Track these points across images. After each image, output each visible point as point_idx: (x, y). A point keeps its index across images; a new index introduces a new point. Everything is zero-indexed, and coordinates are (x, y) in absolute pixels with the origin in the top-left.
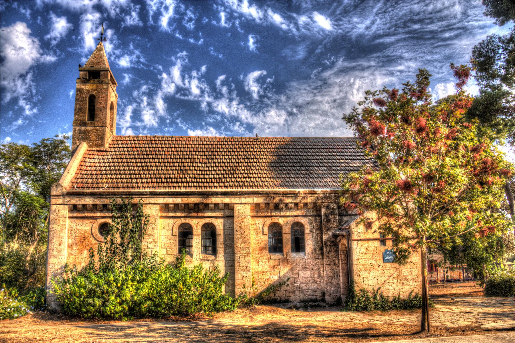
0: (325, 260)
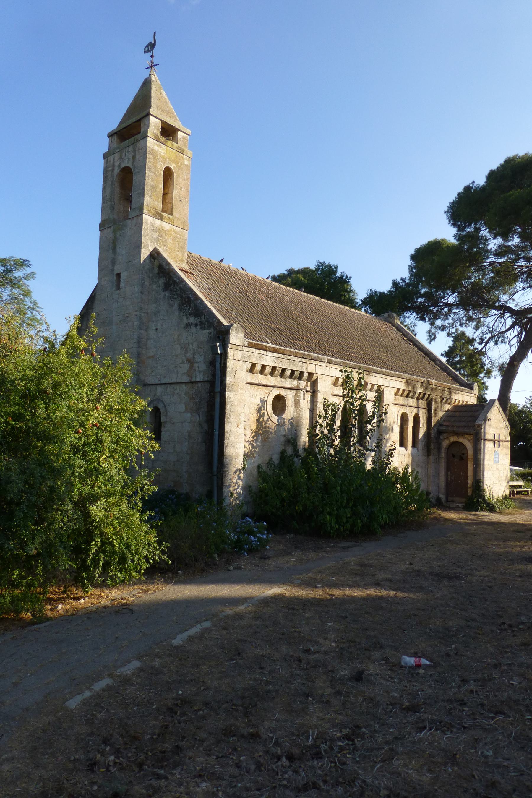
0: (432, 457)
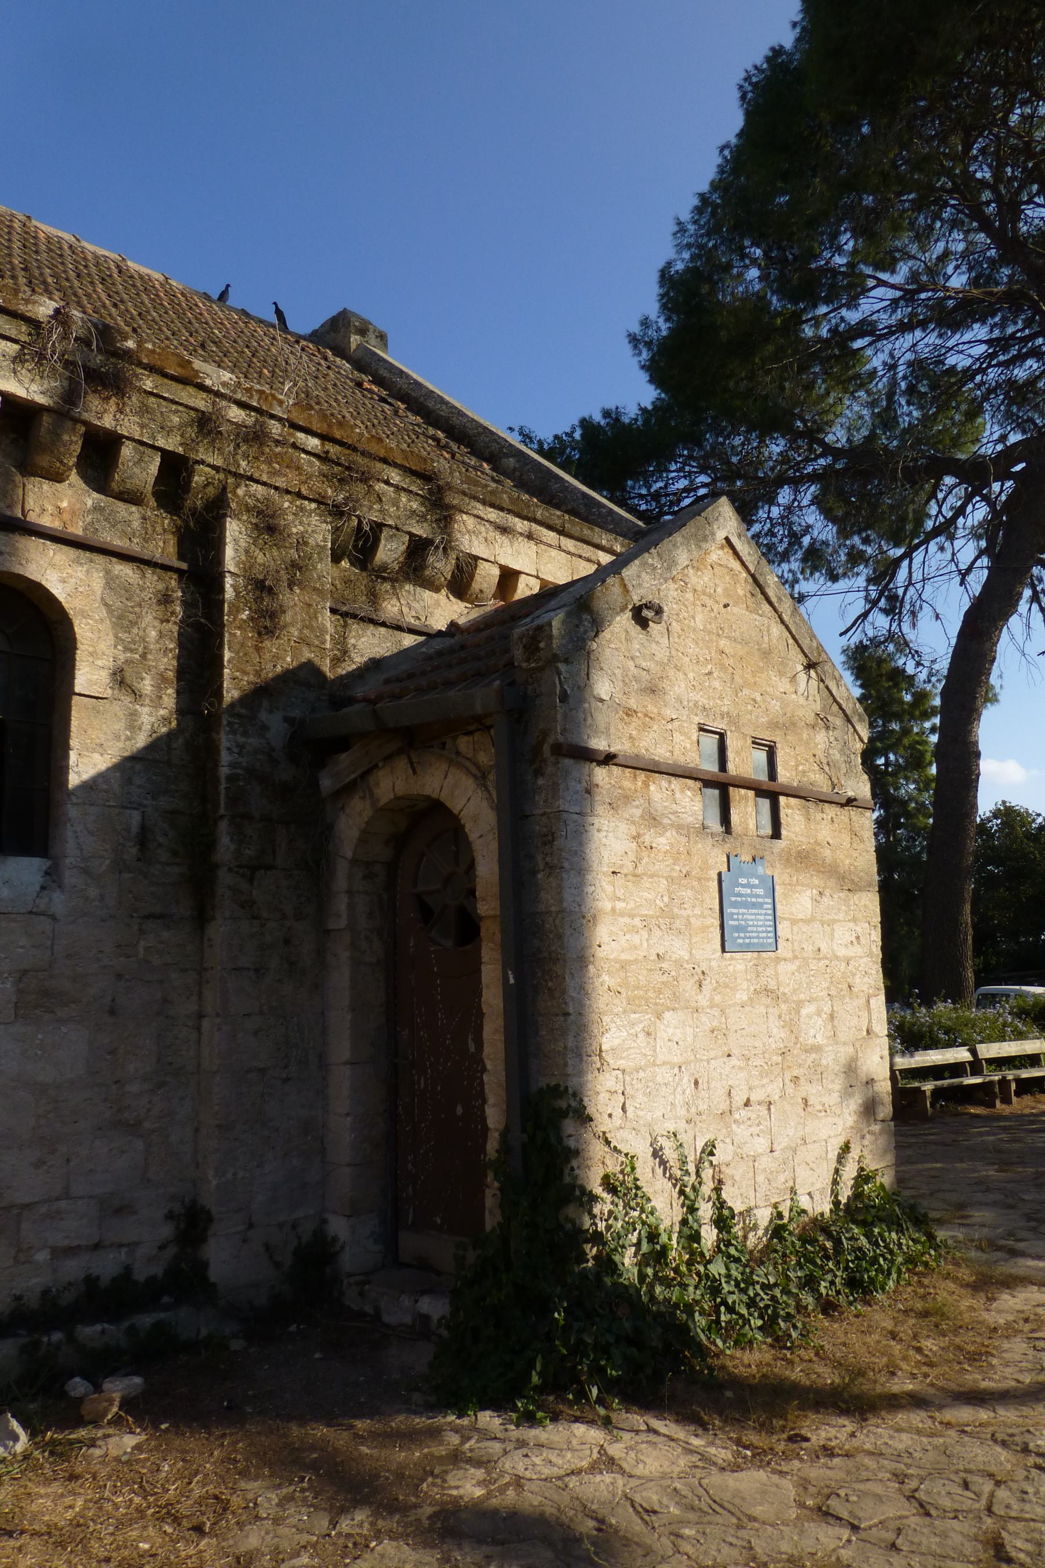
0: (218, 930)
